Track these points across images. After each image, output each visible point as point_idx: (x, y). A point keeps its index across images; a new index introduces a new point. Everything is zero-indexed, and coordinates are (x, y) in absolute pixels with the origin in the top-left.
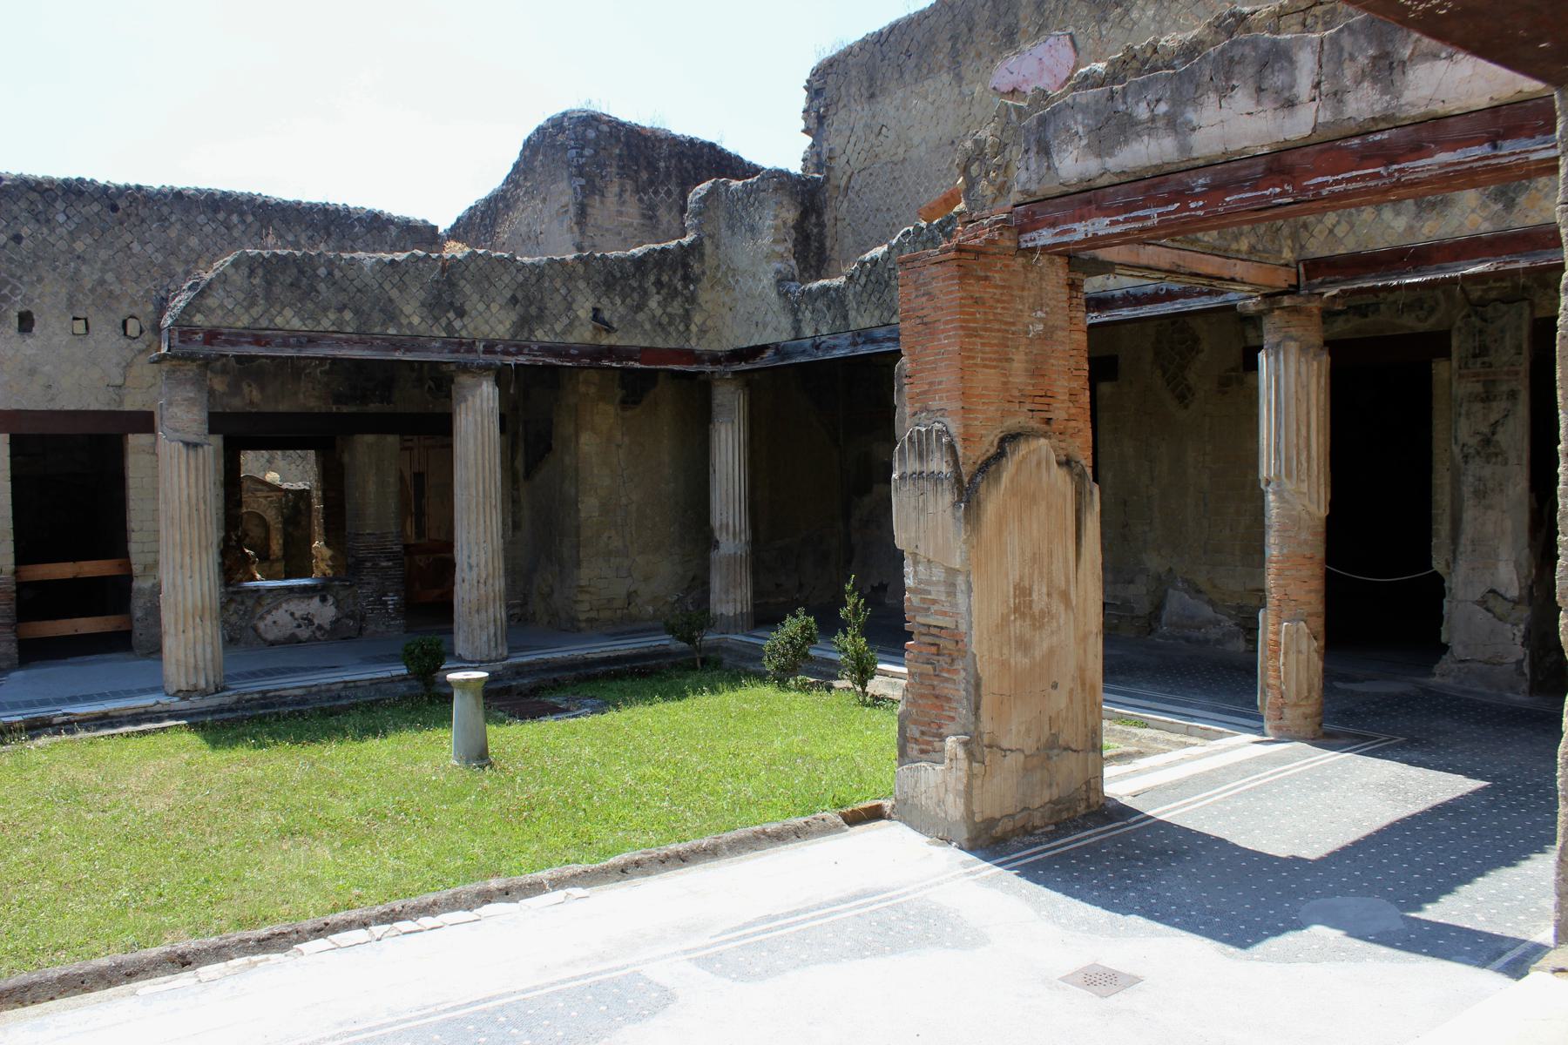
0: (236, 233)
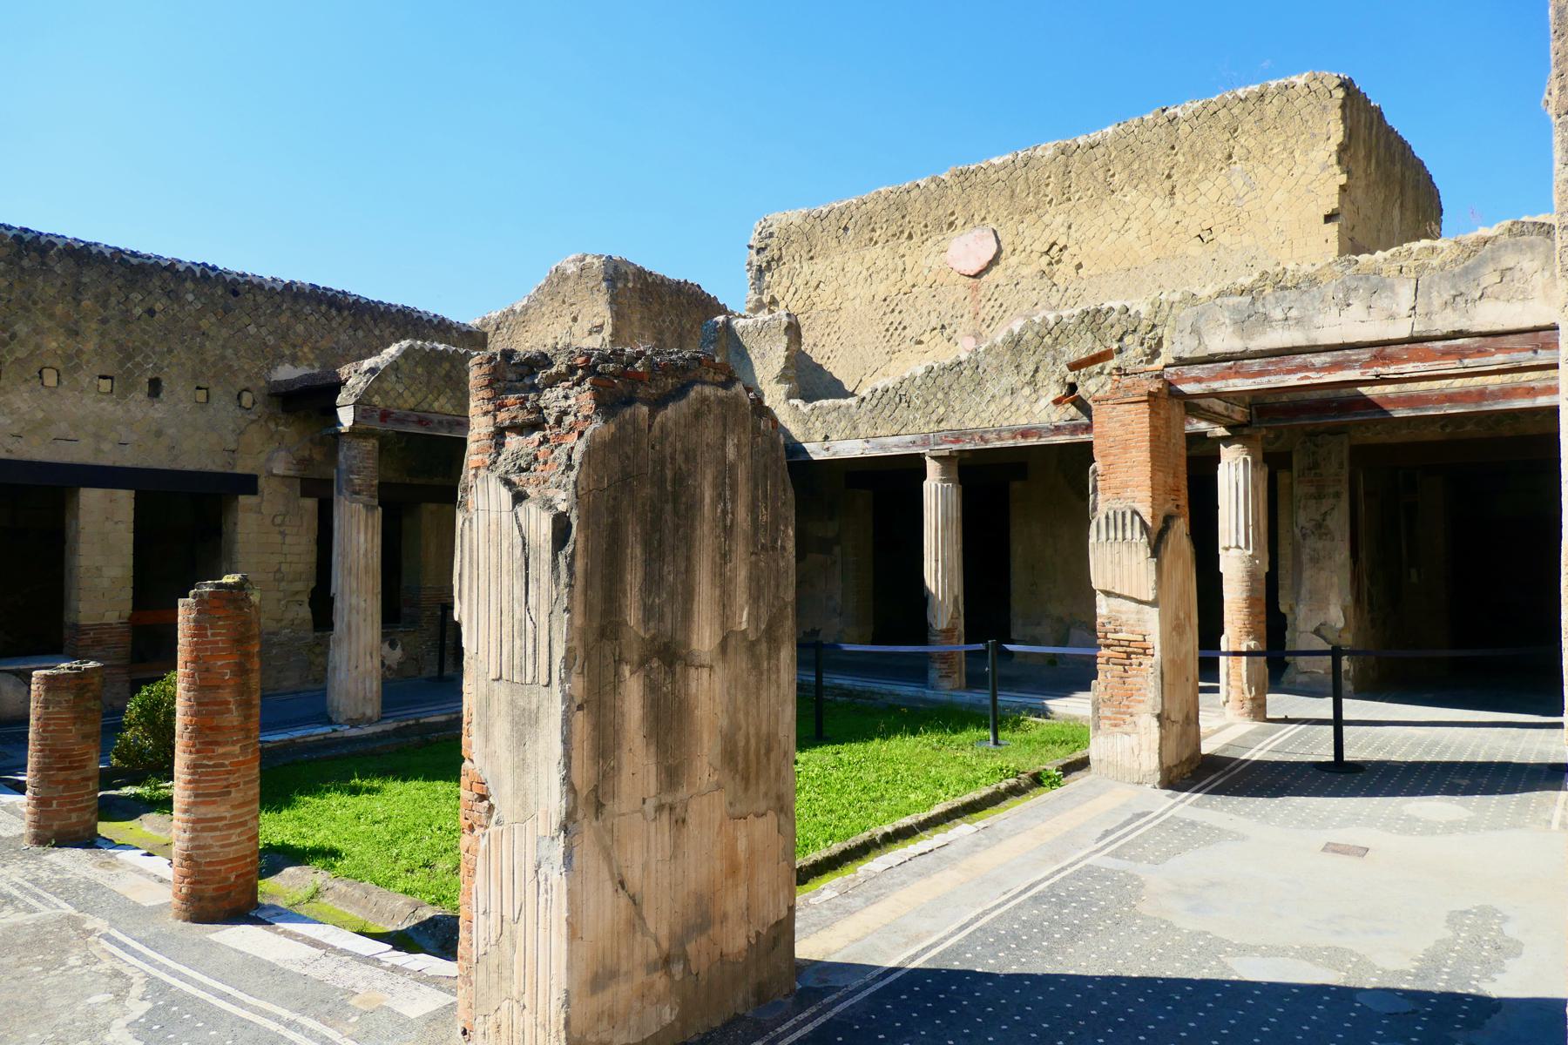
0: (334, 324)
